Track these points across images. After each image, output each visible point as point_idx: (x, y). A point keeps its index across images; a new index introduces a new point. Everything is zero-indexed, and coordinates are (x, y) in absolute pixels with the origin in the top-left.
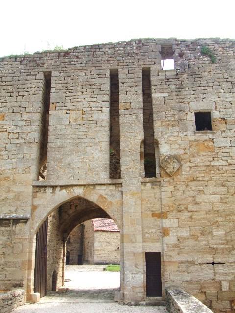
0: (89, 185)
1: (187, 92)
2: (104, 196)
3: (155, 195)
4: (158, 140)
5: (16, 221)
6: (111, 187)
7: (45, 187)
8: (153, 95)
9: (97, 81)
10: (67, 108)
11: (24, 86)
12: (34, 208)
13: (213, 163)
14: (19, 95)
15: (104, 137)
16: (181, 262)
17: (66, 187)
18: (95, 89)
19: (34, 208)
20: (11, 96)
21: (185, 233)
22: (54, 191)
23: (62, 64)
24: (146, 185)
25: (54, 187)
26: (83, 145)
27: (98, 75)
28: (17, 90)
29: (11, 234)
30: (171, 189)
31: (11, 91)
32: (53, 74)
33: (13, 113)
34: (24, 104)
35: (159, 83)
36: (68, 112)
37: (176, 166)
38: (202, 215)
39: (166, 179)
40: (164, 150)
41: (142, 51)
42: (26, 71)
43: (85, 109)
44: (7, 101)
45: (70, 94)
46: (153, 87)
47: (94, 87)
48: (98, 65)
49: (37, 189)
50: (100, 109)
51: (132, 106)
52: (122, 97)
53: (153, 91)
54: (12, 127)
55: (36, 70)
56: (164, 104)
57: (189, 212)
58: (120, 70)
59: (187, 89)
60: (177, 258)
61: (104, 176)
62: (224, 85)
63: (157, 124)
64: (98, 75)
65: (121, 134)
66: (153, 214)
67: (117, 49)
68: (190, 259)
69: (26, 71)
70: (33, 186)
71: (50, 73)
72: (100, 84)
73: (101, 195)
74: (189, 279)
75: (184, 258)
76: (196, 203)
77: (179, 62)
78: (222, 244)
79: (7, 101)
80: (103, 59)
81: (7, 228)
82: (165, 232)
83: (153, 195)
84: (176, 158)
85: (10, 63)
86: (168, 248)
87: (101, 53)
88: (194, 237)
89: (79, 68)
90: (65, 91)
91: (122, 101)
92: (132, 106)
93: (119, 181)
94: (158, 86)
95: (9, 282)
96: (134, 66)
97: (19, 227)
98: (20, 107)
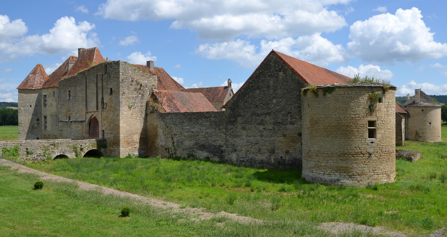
1: (109, 82)
5: (83, 121)
7: (88, 112)
12: (86, 118)
13: (112, 105)
15: (95, 98)
17: (91, 112)
19: (86, 118)
25: (89, 112)
26: (92, 100)
29: (83, 125)
34: (83, 88)
38: (109, 120)
40: (105, 101)
45: (90, 84)
47: (94, 81)
49: (87, 113)
62: (115, 79)
70: (86, 112)
74: (107, 137)
76: (109, 117)
78: (112, 128)
93: (98, 110)
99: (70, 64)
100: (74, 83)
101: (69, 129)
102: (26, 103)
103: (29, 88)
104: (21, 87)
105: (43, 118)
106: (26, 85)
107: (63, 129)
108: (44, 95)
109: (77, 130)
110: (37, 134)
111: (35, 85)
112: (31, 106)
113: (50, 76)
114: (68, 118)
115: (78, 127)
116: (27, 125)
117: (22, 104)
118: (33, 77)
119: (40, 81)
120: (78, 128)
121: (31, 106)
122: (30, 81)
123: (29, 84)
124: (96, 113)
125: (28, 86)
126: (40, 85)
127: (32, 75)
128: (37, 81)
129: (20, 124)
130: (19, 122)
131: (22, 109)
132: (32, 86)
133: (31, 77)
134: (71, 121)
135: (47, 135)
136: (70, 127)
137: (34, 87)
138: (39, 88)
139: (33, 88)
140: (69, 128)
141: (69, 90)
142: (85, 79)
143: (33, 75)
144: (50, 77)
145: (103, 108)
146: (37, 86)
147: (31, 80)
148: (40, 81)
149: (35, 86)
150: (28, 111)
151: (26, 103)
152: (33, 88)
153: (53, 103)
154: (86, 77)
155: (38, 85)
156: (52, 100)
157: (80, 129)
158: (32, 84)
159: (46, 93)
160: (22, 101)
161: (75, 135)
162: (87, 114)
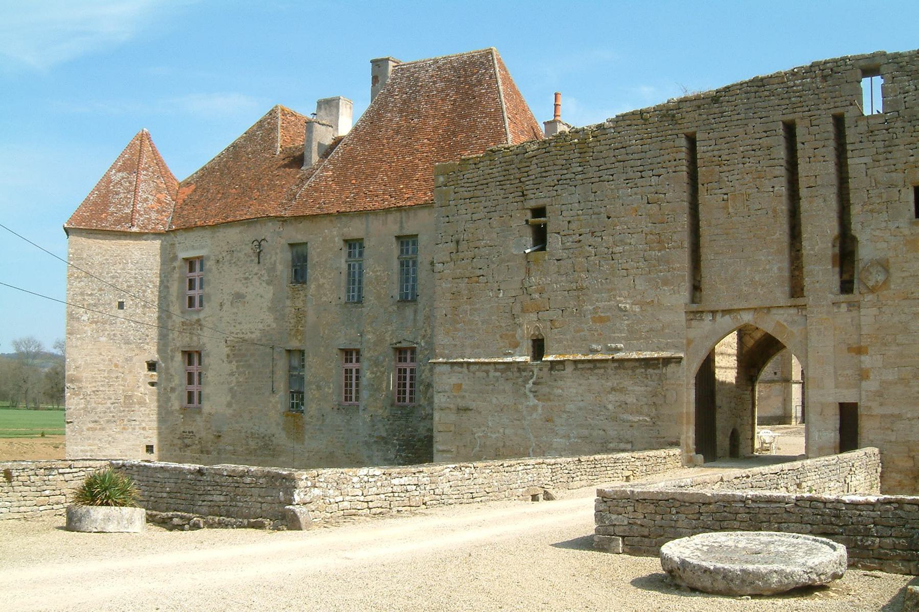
0: (761, 308)
2: (782, 322)
3: (852, 321)
4: (857, 236)
6: (793, 311)
7: (702, 312)
8: (849, 161)
9: (765, 142)
10: (724, 191)
11: (659, 160)
14: (653, 175)
16: (883, 416)
18: (761, 158)
20: (642, 177)
21: (890, 375)
22: (714, 319)
23: (710, 117)
24: (839, 307)
25: (714, 313)
27: (765, 132)
28: (651, 167)
29: (661, 378)
30: (874, 311)
31: (641, 168)
32: (699, 136)
33: (648, 203)
35: (858, 140)
36: (726, 197)
37: (881, 278)
39: (870, 297)
40: (865, 252)
41: (830, 83)
42: (659, 134)
43: (749, 191)
44: (639, 185)
46: (849, 147)
48: (764, 114)
49: (691, 316)
50: (771, 190)
51: (819, 183)
52: (803, 168)
53: (849, 154)
54: (650, 225)
55: (674, 132)
56: (867, 175)
57: (898, 345)
58: (797, 121)
59: (902, 147)
60: (877, 410)
61: (781, 295)
63: (856, 210)
64: (765, 132)
65: (803, 229)
66: (848, 348)
67: (792, 84)
68: (897, 412)
69: (659, 134)
71: (695, 133)
72: (769, 148)
73: (777, 322)
75: (888, 410)
77: (889, 98)
79: (639, 185)
80: (771, 103)
81: (655, 371)
82: (863, 375)
83: (849, 320)
84: (884, 266)
85: (635, 122)
86: (867, 396)
87: (767, 93)
88: (903, 381)
89: (735, 123)
90: (719, 163)
91: (804, 175)
92: (819, 183)
93: (800, 301)
94: (857, 146)
95: (663, 440)
96: (819, 112)
97: (672, 368)
98: (656, 193)
99: (317, 125)
100: (580, 169)
101: (533, 401)
102: (100, 290)
103: (118, 228)
104: (83, 219)
105: (179, 357)
106: (103, 216)
107: (473, 405)
108: (186, 260)
109: (610, 407)
110: (144, 429)
111: (141, 215)
112: (121, 305)
113: (187, 184)
114: (527, 345)
115: (622, 390)
116: (102, 386)
117: (82, 294)
118: (128, 184)
119: (159, 201)
120: (611, 397)
121: (121, 305)
122: (117, 197)
123: (112, 209)
124: (777, 318)
125: (110, 218)
126: (160, 217)
127: (120, 174)
128: (146, 200)
129: (72, 381)
130: (67, 373)
131: (85, 318)
132: (131, 219)
133: (119, 183)
134: (552, 362)
135: (203, 434)
136: (544, 390)
137: (138, 226)
138: (161, 228)
139: (133, 225)
140: (531, 395)
141: (533, 204)
142: (683, 142)
143: (124, 174)
144: (193, 187)
145: (846, 287)
146: (149, 219)
147: (122, 195)
148: (159, 201)
149: (140, 220)
150: (107, 327)
151: (100, 290)
152: (135, 229)
153: (250, 289)
154: (692, 141)
155: (154, 215)
156: (246, 279)
157: (631, 399)
158: (128, 211)
159: (202, 247)
160: (82, 283)
161: (585, 432)
162: (694, 323)
